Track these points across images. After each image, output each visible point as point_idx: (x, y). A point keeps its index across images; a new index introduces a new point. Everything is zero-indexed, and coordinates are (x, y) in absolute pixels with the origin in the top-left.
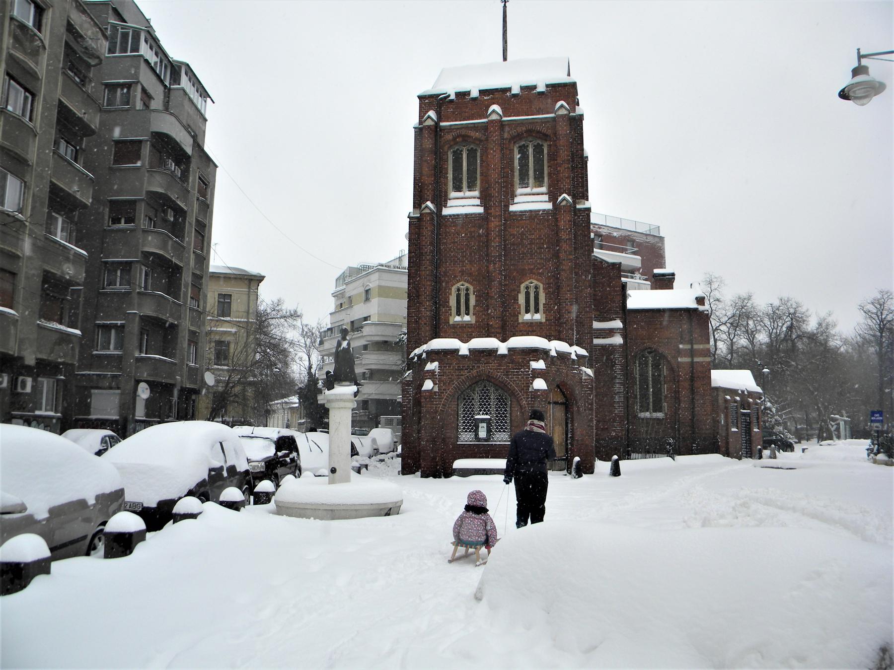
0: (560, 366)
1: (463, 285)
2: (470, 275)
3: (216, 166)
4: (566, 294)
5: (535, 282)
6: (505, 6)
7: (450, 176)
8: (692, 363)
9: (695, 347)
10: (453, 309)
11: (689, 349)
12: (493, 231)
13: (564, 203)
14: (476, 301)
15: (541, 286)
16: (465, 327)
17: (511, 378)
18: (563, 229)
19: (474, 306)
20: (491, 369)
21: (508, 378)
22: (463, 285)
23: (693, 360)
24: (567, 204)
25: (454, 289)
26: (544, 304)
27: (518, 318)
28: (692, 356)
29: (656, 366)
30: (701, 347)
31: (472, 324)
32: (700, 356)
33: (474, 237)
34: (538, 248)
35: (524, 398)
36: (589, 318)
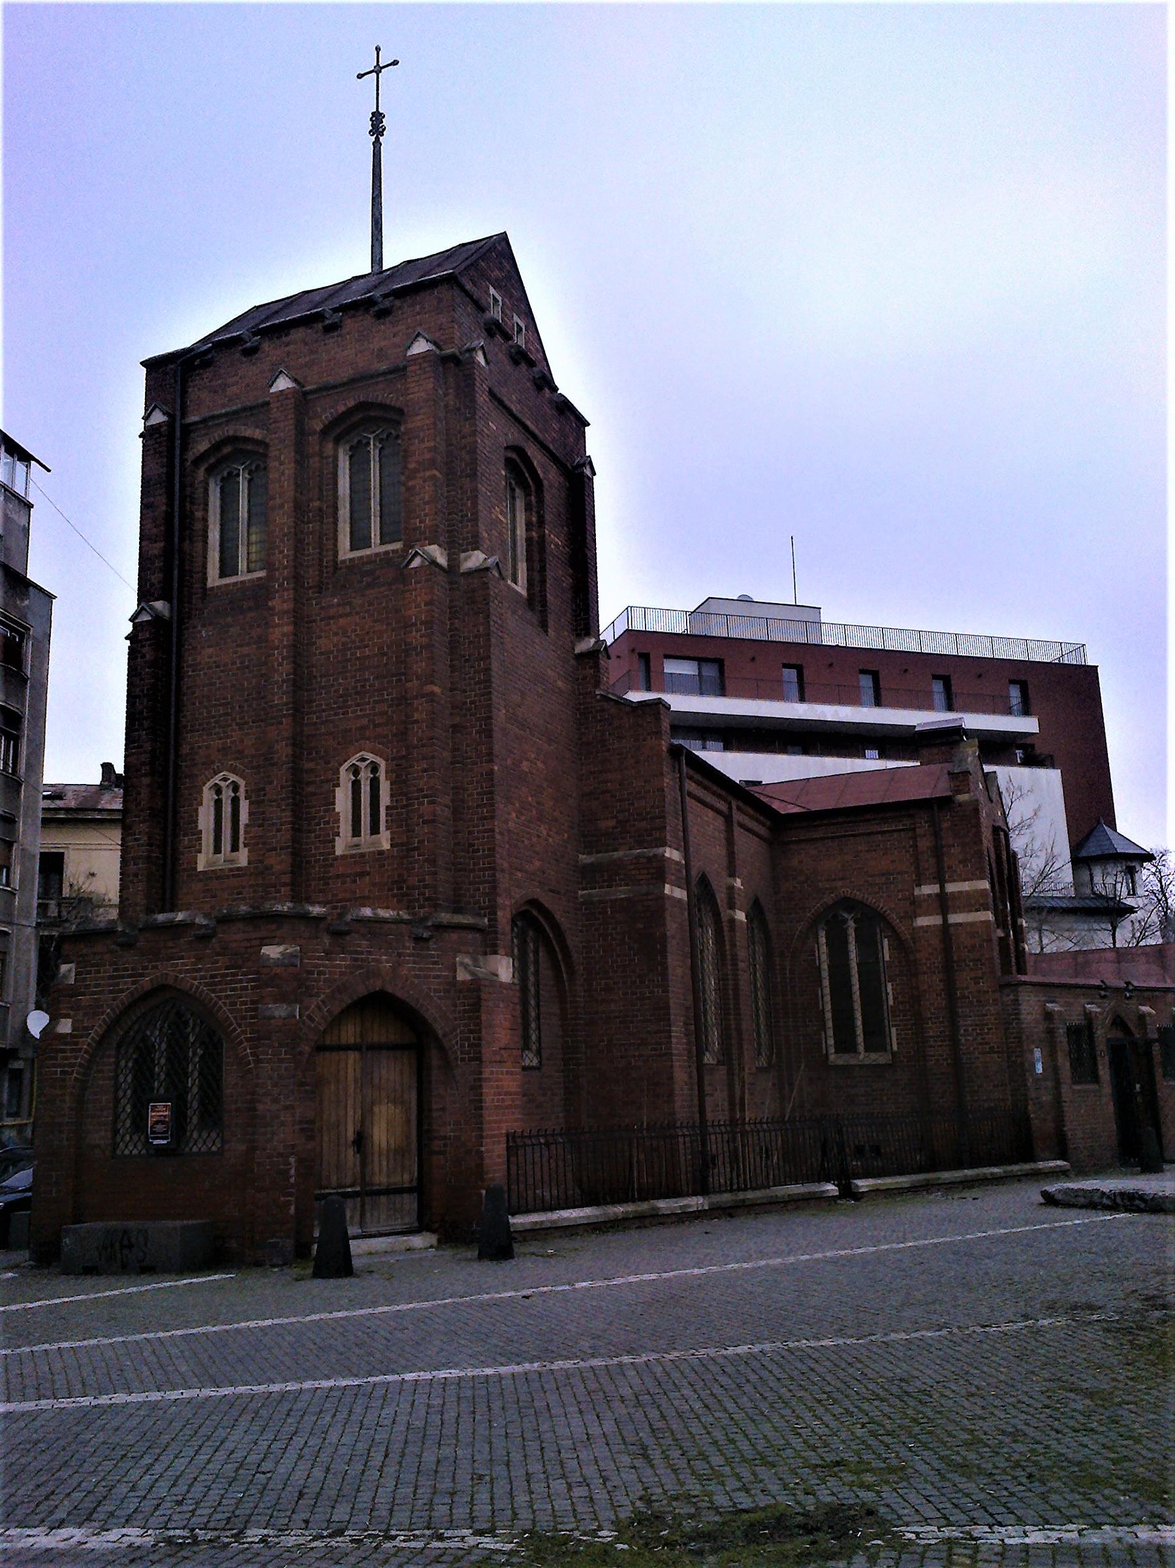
0: (370, 953)
1: (224, 778)
2: (240, 756)
3: (50, 597)
4: (421, 778)
5: (371, 757)
6: (377, 145)
7: (214, 536)
8: (946, 925)
9: (951, 888)
10: (204, 835)
11: (937, 895)
12: (277, 648)
13: (416, 563)
14: (251, 814)
15: (383, 765)
16: (228, 877)
17: (221, 991)
18: (415, 624)
19: (247, 826)
20: (180, 972)
21: (214, 991)
22: (225, 779)
23: (945, 920)
24: (422, 562)
25: (205, 789)
26: (387, 807)
27: (334, 847)
28: (944, 911)
29: (868, 945)
30: (965, 886)
31: (239, 869)
32: (960, 909)
33: (247, 667)
34: (376, 678)
35: (248, 1040)
36: (486, 831)
